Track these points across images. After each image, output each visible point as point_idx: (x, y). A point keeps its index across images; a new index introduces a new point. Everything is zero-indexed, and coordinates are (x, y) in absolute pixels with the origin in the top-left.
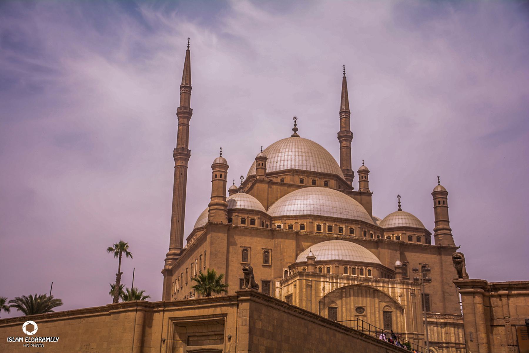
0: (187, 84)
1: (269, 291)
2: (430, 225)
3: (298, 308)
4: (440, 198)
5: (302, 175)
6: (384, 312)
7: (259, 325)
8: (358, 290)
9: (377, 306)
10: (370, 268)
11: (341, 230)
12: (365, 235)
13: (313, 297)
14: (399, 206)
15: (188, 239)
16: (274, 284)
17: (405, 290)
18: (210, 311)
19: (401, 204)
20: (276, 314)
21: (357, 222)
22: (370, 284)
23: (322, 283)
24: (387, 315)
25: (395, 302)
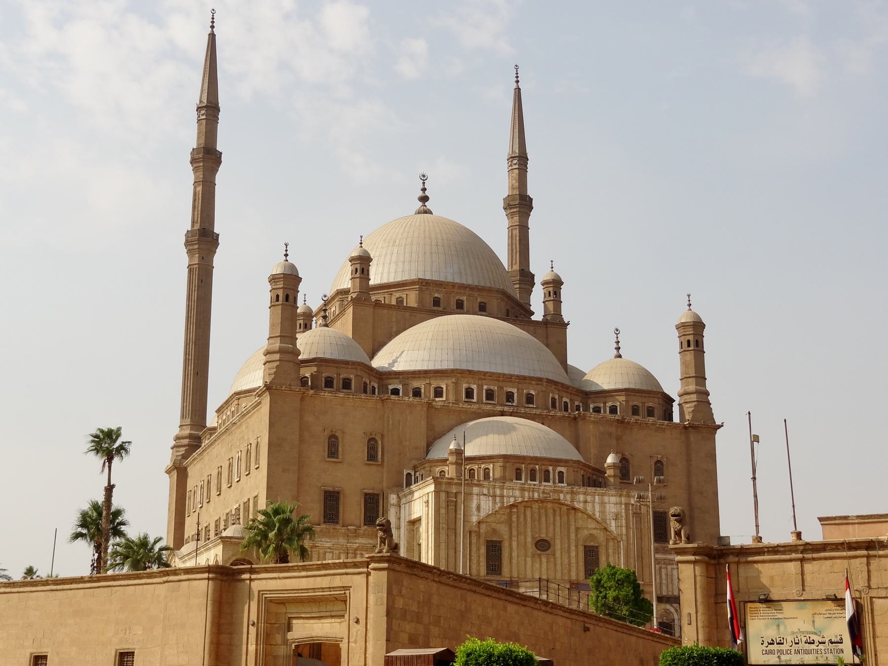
2: (672, 386)
3: (452, 573)
4: (693, 336)
5: (438, 291)
6: (585, 547)
7: (400, 603)
8: (539, 508)
9: (573, 536)
11: (510, 397)
12: (554, 406)
14: (618, 349)
15: (219, 411)
16: (385, 498)
17: (623, 506)
18: (325, 582)
20: (422, 585)
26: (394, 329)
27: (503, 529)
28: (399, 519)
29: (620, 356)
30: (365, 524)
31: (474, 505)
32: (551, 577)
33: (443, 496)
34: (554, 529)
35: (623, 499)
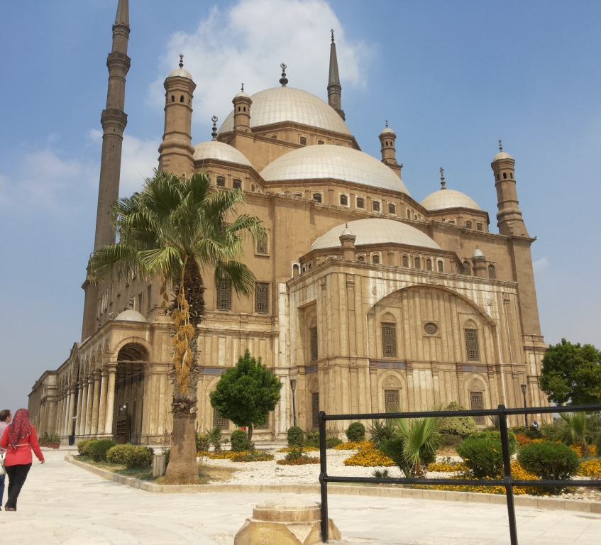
0: (123, 23)
1: (267, 299)
6: (466, 330)
9: (455, 320)
10: (441, 259)
11: (376, 206)
12: (409, 216)
13: (358, 304)
16: (275, 288)
17: (496, 294)
19: (444, 181)
21: (398, 194)
22: (445, 283)
23: (371, 280)
24: (471, 335)
25: (481, 314)
26: (271, 158)
27: (396, 312)
28: (289, 306)
29: (445, 189)
30: (256, 311)
31: (371, 288)
32: (440, 360)
33: (342, 277)
34: (439, 313)
35: (495, 288)
